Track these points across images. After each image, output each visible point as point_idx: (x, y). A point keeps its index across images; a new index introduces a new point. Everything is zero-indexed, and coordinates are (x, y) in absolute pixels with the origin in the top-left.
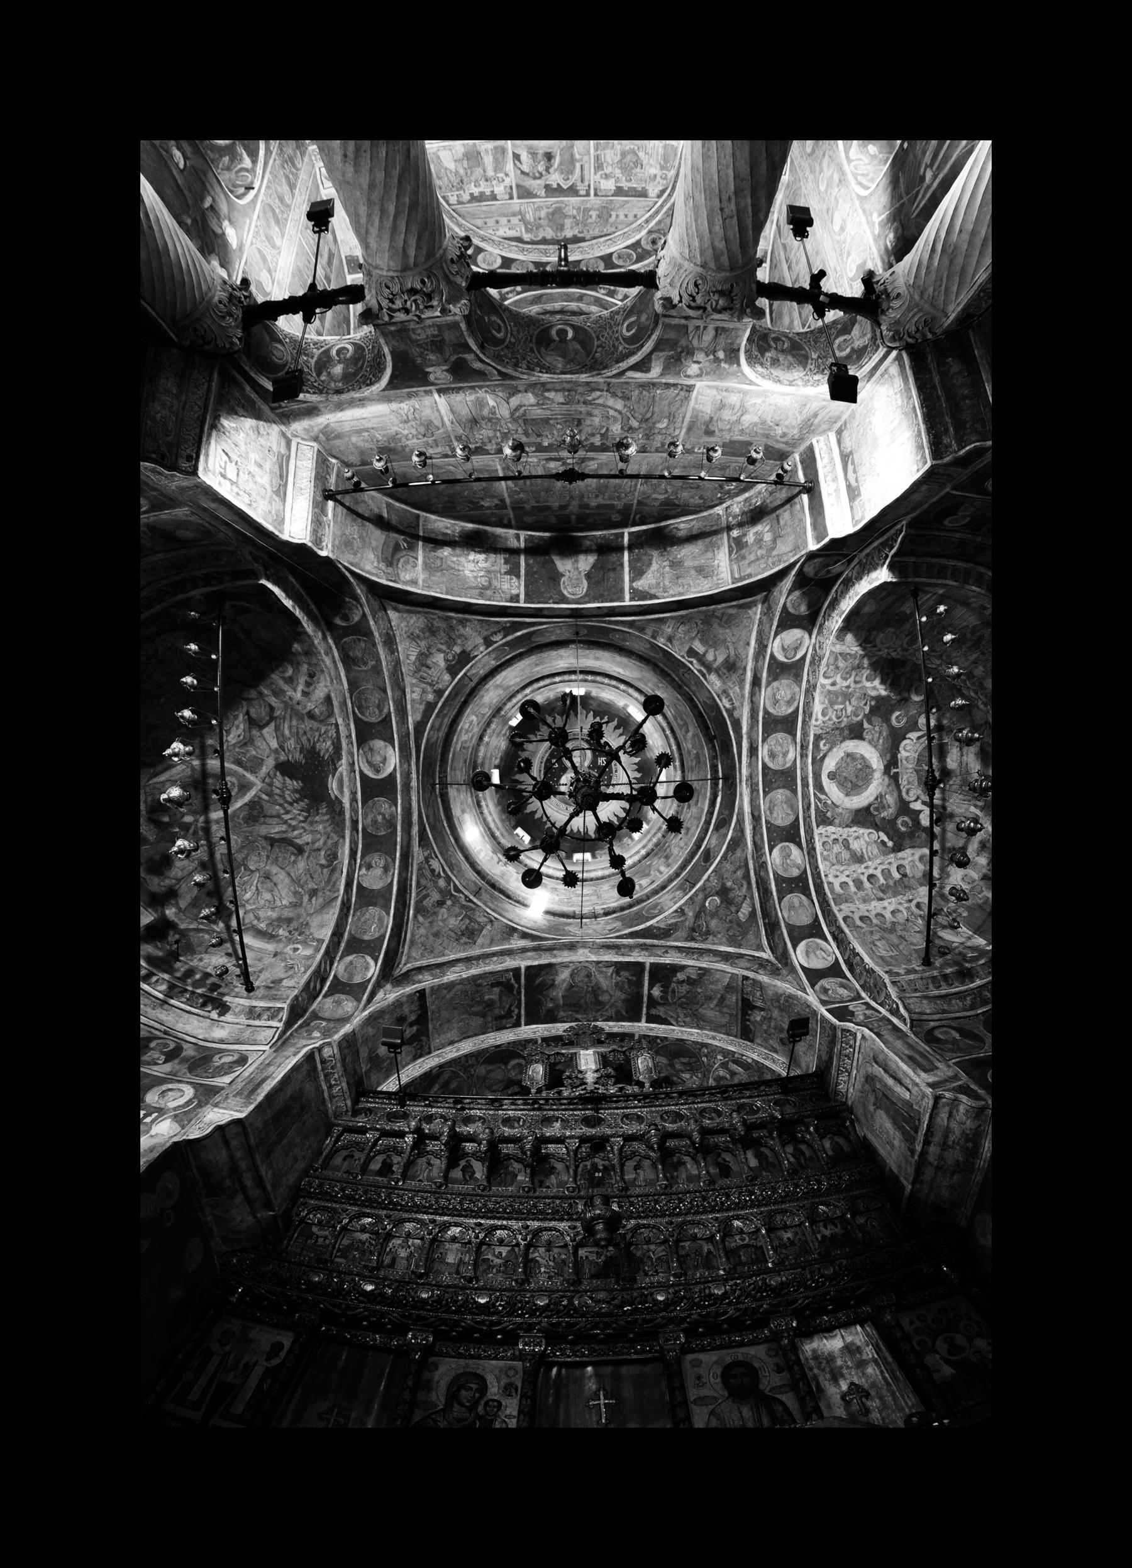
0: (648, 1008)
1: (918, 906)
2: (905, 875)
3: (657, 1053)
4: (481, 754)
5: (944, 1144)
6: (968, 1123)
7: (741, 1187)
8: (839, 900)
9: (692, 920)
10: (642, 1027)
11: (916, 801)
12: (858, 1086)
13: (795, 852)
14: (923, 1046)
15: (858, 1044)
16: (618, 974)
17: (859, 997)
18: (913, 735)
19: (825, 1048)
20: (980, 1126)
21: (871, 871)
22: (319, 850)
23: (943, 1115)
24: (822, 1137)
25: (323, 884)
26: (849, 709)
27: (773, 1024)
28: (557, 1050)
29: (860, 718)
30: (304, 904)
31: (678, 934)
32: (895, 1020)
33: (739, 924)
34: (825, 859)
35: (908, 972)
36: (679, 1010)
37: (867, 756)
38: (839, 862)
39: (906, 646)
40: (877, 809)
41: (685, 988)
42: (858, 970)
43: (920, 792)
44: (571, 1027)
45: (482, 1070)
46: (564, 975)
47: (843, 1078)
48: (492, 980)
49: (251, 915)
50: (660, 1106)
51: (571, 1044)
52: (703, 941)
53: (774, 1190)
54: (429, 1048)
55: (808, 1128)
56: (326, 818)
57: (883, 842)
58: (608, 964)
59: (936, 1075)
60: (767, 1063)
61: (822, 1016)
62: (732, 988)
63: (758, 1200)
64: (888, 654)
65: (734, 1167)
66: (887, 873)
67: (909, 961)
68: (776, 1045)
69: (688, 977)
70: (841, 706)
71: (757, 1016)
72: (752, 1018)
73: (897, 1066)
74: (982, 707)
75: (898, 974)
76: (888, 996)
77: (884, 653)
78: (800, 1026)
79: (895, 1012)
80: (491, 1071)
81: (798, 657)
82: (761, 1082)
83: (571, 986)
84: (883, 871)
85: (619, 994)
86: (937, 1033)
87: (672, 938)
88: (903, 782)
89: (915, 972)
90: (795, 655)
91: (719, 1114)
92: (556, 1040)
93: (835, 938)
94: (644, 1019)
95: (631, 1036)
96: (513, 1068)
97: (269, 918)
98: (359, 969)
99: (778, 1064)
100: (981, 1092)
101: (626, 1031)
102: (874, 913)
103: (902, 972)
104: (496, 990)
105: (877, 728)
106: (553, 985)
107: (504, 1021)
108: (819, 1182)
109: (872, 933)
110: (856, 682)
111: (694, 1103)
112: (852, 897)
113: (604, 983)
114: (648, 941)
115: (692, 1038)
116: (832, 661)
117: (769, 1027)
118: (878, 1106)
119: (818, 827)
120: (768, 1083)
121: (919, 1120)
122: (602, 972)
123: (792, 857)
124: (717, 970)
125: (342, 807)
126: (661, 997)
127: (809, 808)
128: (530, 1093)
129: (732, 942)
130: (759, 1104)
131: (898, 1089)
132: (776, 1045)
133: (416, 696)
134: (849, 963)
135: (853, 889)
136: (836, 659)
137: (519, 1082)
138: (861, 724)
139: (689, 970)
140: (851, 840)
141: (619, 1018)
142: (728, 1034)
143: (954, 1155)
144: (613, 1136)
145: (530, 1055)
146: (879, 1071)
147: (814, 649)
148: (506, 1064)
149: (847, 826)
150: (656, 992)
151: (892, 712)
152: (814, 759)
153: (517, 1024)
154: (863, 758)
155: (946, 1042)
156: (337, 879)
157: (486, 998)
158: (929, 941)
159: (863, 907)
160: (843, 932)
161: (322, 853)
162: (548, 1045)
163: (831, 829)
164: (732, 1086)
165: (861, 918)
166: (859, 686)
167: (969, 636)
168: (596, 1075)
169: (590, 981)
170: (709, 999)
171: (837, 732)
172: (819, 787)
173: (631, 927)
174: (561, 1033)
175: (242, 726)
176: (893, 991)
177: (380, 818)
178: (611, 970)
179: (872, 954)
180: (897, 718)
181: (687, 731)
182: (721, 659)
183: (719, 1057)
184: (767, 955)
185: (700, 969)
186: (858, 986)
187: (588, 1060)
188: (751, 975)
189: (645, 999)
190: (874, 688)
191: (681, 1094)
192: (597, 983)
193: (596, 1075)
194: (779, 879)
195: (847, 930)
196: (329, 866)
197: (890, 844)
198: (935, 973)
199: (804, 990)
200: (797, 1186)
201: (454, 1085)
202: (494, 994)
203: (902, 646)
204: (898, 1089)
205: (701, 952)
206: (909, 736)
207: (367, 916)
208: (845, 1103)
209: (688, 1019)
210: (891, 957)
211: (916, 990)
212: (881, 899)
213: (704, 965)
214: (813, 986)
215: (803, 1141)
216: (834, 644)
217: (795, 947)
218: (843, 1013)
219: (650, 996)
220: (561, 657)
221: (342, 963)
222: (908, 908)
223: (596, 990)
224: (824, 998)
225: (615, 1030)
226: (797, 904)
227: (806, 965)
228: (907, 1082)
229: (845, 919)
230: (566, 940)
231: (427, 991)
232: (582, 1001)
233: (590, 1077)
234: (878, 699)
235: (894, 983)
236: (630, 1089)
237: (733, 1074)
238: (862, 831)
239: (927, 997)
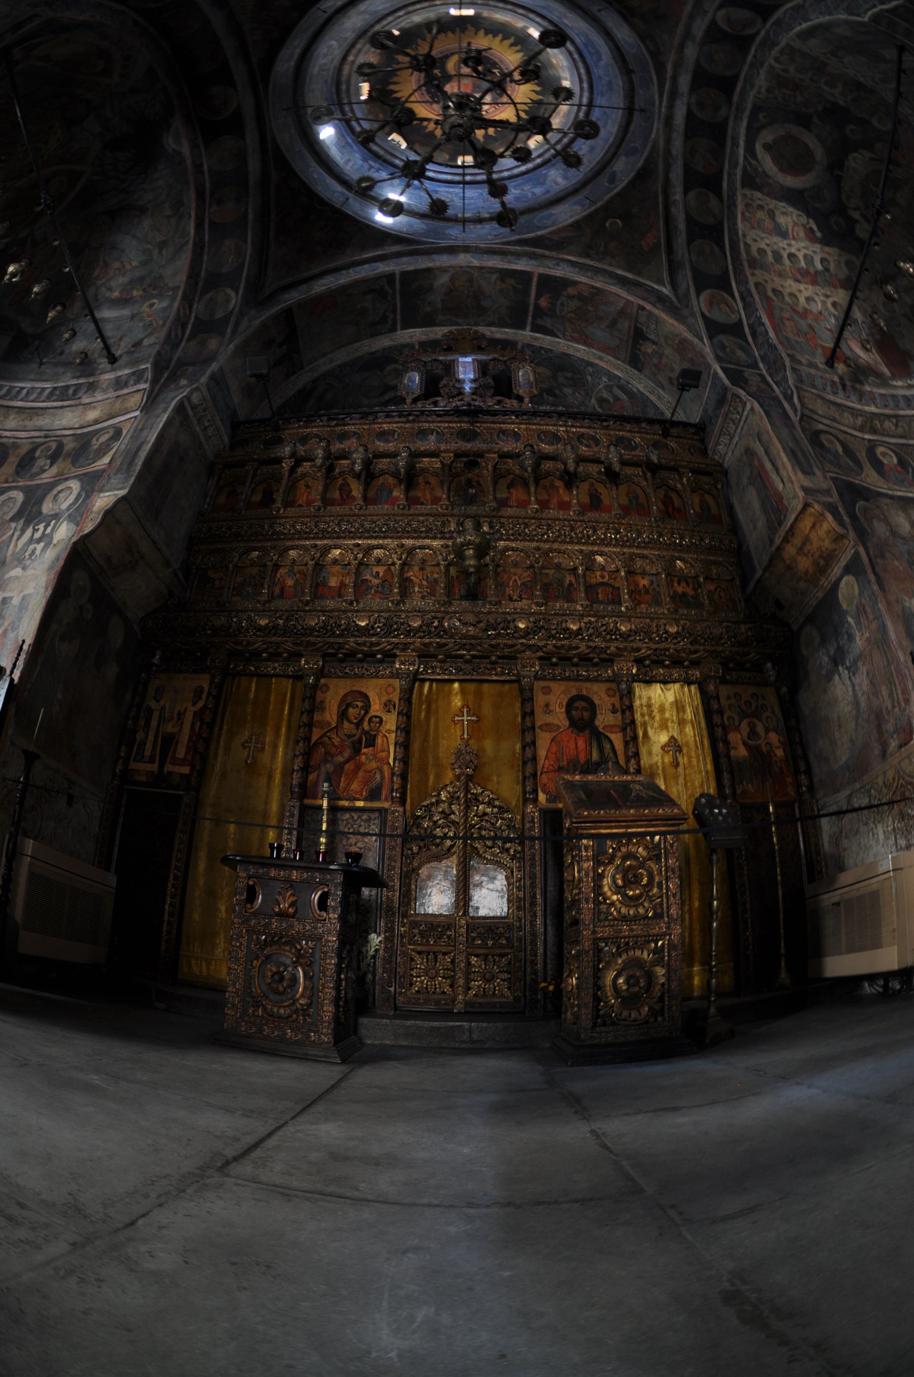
230: (444, 243)
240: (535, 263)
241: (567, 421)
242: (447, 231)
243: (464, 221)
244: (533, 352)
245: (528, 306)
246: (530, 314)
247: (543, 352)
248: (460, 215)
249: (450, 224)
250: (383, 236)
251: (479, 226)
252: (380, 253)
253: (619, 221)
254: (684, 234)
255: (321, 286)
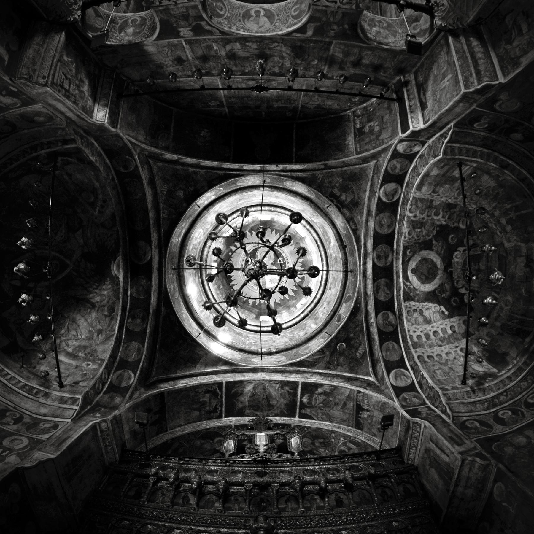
0: (300, 409)
1: (461, 350)
2: (454, 332)
3: (304, 437)
4: (205, 253)
5: (466, 486)
6: (480, 473)
7: (348, 513)
8: (415, 346)
9: (328, 357)
10: (296, 420)
11: (462, 288)
12: (421, 455)
13: (391, 317)
14: (458, 431)
15: (422, 431)
16: (282, 387)
17: (425, 403)
18: (461, 249)
19: (403, 434)
20: (486, 475)
21: (435, 329)
22: (104, 306)
23: (466, 470)
24: (398, 484)
25: (106, 327)
26: (424, 232)
27: (374, 419)
28: (242, 432)
29: (430, 237)
30: (94, 338)
31: (320, 365)
32: (444, 416)
33: (357, 360)
34: (408, 321)
35: (453, 388)
36: (319, 411)
37: (434, 260)
38: (417, 323)
39: (456, 196)
40: (440, 292)
41: (322, 398)
42: (425, 387)
43: (464, 283)
44: (253, 419)
45: (198, 443)
46: (249, 388)
47: (413, 450)
48: (205, 389)
49: (64, 343)
50: (303, 466)
51: (252, 429)
52: (334, 370)
53: (368, 514)
54: (166, 428)
55: (390, 479)
56: (109, 287)
57: (443, 312)
58: (277, 382)
59: (465, 448)
60: (370, 443)
61: (402, 415)
62: (351, 398)
63: (358, 520)
64: (447, 200)
65: (346, 501)
66: (444, 331)
67: (454, 382)
68: (376, 432)
69: (324, 391)
70: (419, 230)
71: (365, 415)
72: (362, 416)
73: (443, 443)
74: (499, 234)
75: (447, 390)
76: (441, 402)
77: (444, 199)
78: (388, 420)
79: (444, 412)
80: (203, 444)
81: (396, 198)
82: (365, 453)
83: (254, 395)
84: (442, 329)
85: (282, 400)
86: (468, 424)
87: (316, 368)
88: (455, 276)
89: (457, 388)
90: (393, 198)
91: (338, 471)
92: (243, 427)
93: (413, 368)
94: (297, 416)
95: (289, 426)
96: (217, 442)
97: (74, 346)
98: (125, 378)
99: (375, 443)
100: (488, 456)
101: (286, 422)
102: (436, 353)
103: (449, 388)
104: (208, 395)
105: (440, 244)
106: (242, 394)
107: (212, 414)
108: (394, 510)
109: (434, 365)
110: (428, 216)
111: (323, 465)
112: (423, 344)
113: (274, 393)
114: (301, 369)
115: (326, 428)
116: (414, 202)
117: (372, 421)
118: (431, 466)
119: (405, 301)
120: (369, 454)
121: (453, 473)
122: (272, 387)
123: (389, 320)
124: (342, 387)
125: (119, 281)
126: (308, 403)
127: (400, 290)
128: (225, 456)
129: (351, 371)
130: (362, 465)
131: (443, 456)
132: (376, 432)
133: (165, 216)
134: (420, 383)
135: (424, 339)
136: (416, 201)
137: (219, 451)
138: (431, 240)
139: (325, 387)
140: (424, 310)
141: (282, 415)
142: (347, 426)
143: (470, 492)
144: (274, 482)
145: (226, 435)
146: (432, 446)
147: (404, 196)
148: (213, 440)
149: (422, 302)
150: (305, 400)
151: (449, 235)
152: (403, 261)
153: (220, 417)
154: (432, 261)
155: (471, 428)
156: (114, 325)
157: (201, 400)
158: (465, 370)
159: (430, 350)
160: (417, 365)
161: (106, 308)
162: (238, 429)
163: (413, 303)
164: (347, 455)
165: (428, 357)
166: (430, 218)
167: (491, 192)
168: (265, 448)
169: (265, 392)
170: (337, 404)
171: (417, 245)
172: (406, 278)
173: (291, 360)
174: (246, 423)
175: (64, 231)
176: (443, 399)
177: (141, 289)
178: (278, 385)
179: (433, 377)
180: (452, 238)
181: (330, 243)
182: (349, 200)
183: (342, 439)
184: (371, 379)
185: (332, 386)
186: (424, 397)
187: (261, 439)
188: (362, 390)
189: (298, 404)
190: (439, 220)
191: (316, 459)
192: (270, 393)
193: (265, 448)
194: (380, 332)
195: (419, 364)
196: (109, 316)
197: (447, 313)
198: (469, 389)
199: (392, 400)
200: (381, 512)
201: (181, 450)
202: (206, 398)
203: (454, 196)
204: (443, 456)
205: (333, 376)
206: (458, 249)
207: (131, 347)
208: (413, 465)
209: (324, 417)
210: (444, 380)
211: (457, 399)
212: (440, 346)
213: (335, 384)
214: (398, 396)
215: (387, 487)
216: (415, 193)
217: (388, 374)
218: (414, 413)
219: (301, 402)
220: (255, 195)
221: (115, 375)
222: (456, 351)
223: (268, 398)
224: (404, 404)
225: (280, 422)
226: (391, 348)
227: (394, 384)
228: (447, 451)
229: (419, 357)
231: (166, 395)
232: (260, 404)
233: (262, 449)
234: (441, 226)
235: (444, 395)
236: (285, 457)
237: (350, 449)
238: (430, 305)
239: (463, 403)
240: (299, 376)
241: (319, 463)
242: (253, 360)
243: (262, 354)
244: (300, 430)
245: (297, 403)
246: (298, 407)
247: (306, 429)
248: (260, 351)
249: (254, 356)
250: (219, 361)
251: (270, 357)
252: (215, 369)
253: (343, 344)
254: (378, 342)
255: (182, 384)
